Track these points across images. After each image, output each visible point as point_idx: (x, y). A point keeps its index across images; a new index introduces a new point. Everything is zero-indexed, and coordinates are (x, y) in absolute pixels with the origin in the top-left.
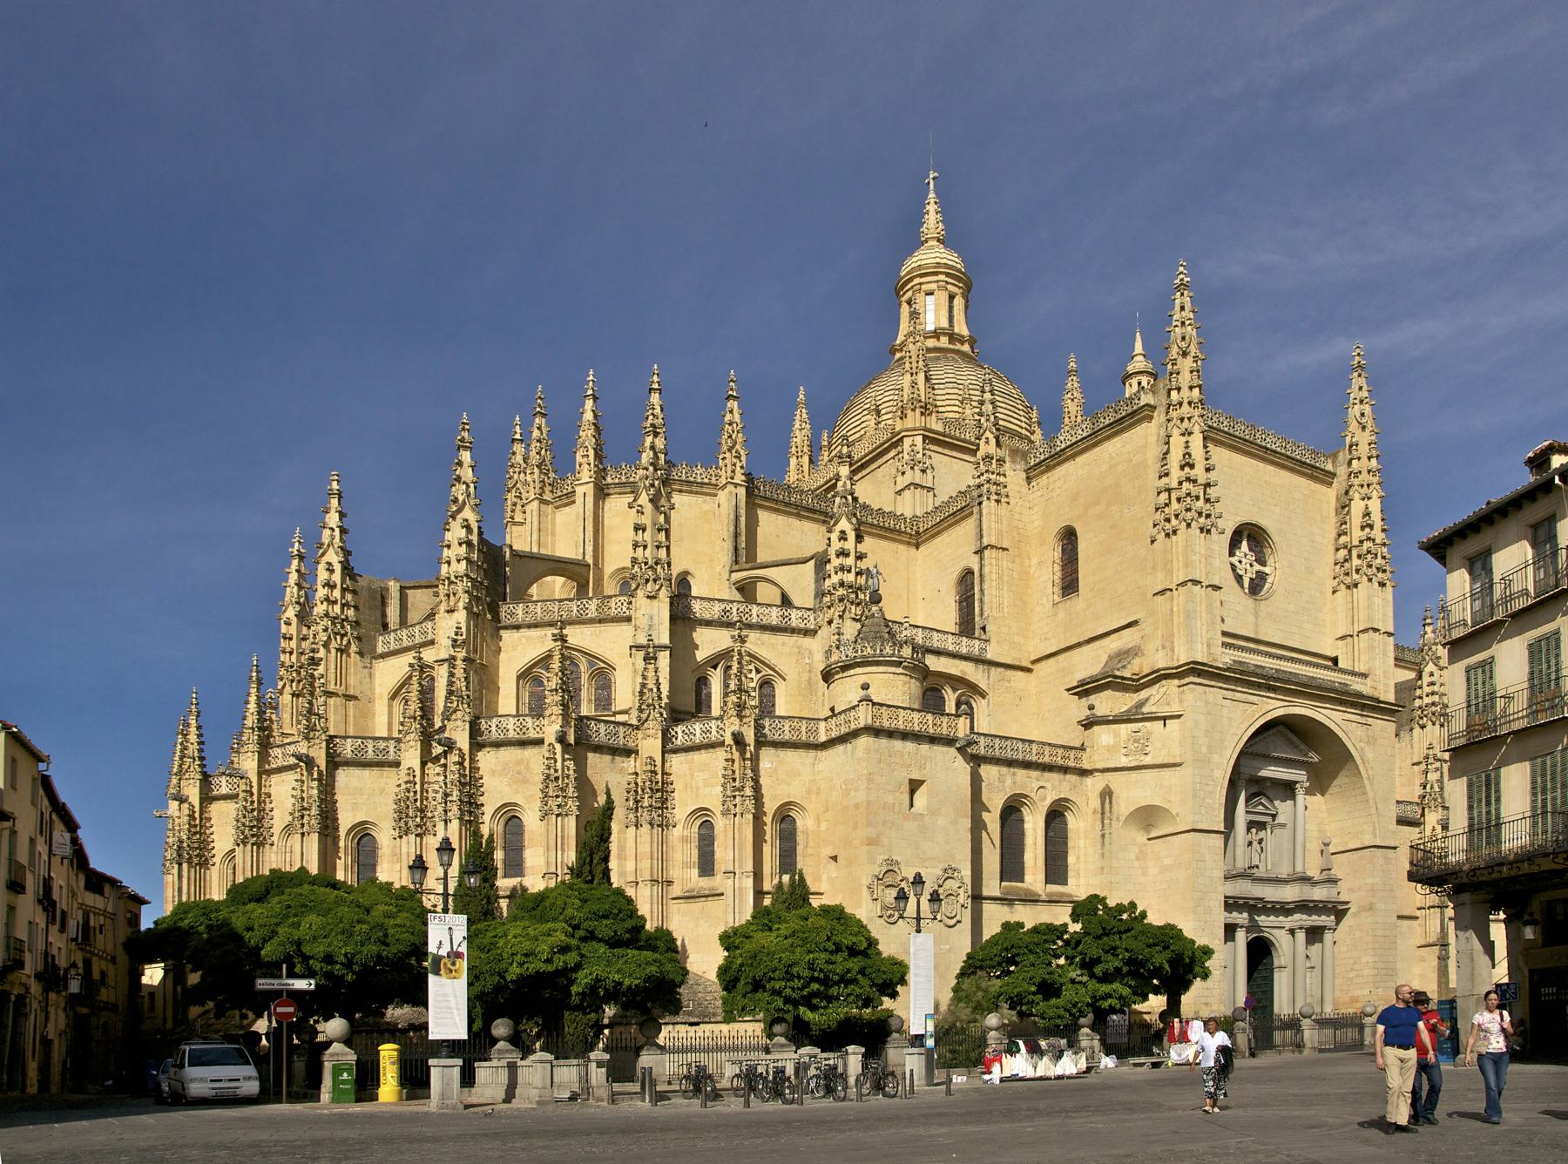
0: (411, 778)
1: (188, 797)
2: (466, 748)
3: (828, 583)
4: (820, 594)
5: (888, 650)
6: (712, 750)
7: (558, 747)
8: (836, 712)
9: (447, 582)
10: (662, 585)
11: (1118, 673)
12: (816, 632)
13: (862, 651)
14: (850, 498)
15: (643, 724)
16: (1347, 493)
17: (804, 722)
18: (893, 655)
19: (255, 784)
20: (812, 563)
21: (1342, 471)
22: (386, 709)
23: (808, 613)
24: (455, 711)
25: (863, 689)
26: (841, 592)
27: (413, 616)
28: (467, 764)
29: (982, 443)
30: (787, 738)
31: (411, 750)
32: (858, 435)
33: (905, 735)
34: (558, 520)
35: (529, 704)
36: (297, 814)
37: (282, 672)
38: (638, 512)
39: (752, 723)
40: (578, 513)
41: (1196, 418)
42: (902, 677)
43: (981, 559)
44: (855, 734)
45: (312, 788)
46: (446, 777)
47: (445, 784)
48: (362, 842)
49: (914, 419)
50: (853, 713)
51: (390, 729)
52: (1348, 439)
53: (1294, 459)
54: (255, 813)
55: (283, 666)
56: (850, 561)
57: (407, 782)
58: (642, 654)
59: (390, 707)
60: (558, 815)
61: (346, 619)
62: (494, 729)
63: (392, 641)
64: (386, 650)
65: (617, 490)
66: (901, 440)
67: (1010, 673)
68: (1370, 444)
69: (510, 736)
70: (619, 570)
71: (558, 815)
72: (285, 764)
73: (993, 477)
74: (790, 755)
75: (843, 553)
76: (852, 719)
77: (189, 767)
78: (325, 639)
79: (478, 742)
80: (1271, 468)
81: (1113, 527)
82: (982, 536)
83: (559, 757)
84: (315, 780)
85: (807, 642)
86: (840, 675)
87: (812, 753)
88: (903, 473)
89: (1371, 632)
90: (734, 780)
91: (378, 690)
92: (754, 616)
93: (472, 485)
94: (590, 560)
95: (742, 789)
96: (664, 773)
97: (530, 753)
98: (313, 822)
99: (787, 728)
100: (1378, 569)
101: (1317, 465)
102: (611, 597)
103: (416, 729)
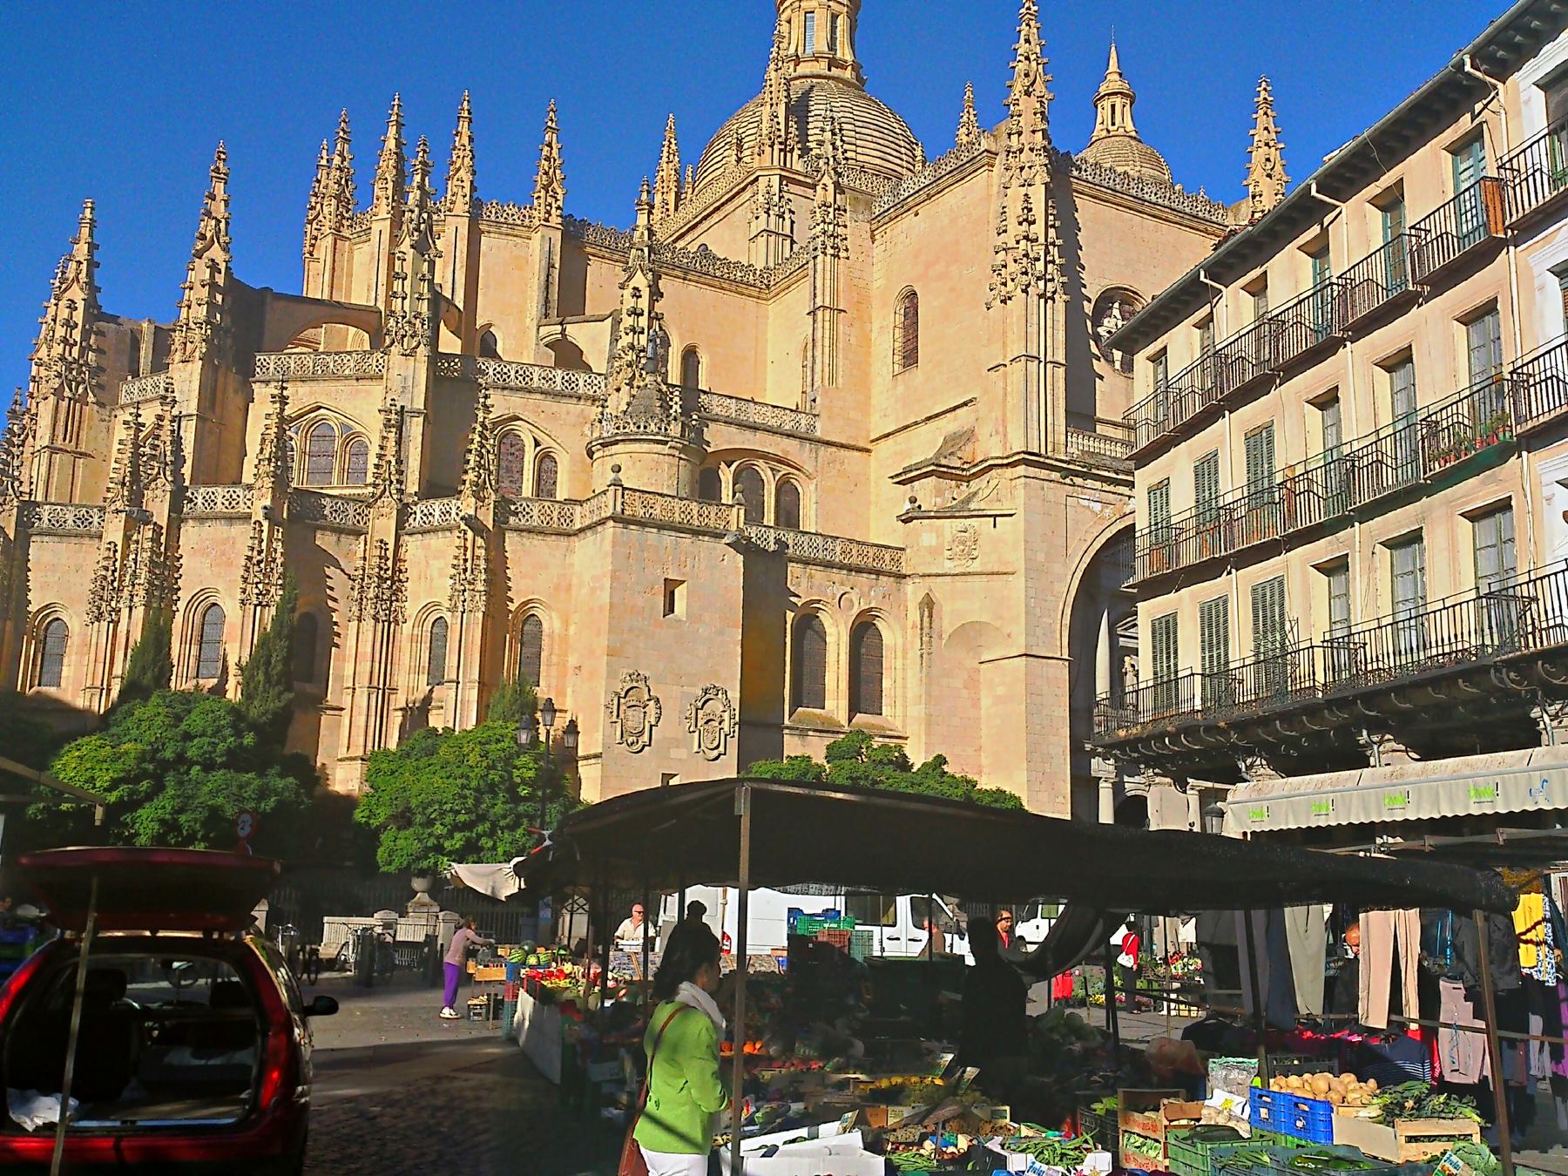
9: (184, 329)
11: (943, 462)
32: (718, 172)
39: (492, 506)
41: (1038, 167)
44: (602, 522)
48: (51, 628)
66: (756, 179)
67: (843, 452)
76: (603, 505)
81: (952, 289)
88: (757, 218)
96: (396, 559)
99: (535, 513)
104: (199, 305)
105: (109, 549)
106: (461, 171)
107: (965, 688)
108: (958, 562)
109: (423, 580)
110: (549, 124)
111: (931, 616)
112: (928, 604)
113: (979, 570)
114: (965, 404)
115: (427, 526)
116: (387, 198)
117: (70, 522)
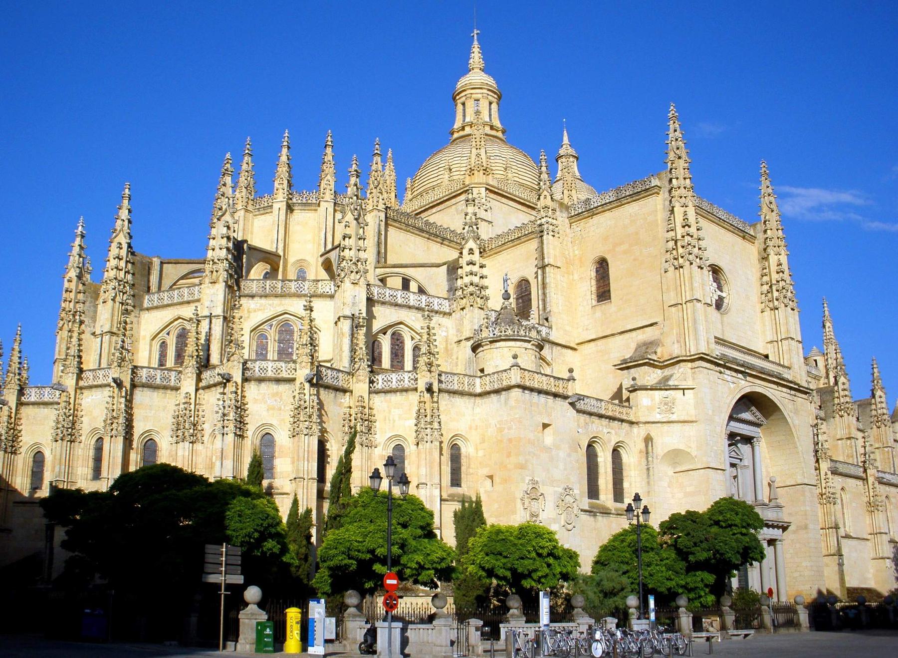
1: (8, 402)
2: (239, 381)
3: (459, 283)
4: (452, 290)
5: (522, 333)
6: (404, 393)
7: (307, 385)
8: (486, 373)
10: (361, 276)
13: (505, 332)
14: (475, 227)
15: (356, 372)
16: (765, 250)
17: (466, 378)
18: (525, 336)
19: (72, 396)
20: (445, 267)
21: (761, 236)
22: (148, 347)
24: (233, 355)
25: (514, 358)
26: (472, 289)
27: (166, 283)
28: (239, 392)
29: (542, 198)
30: (456, 389)
32: (435, 183)
33: (540, 392)
34: (255, 224)
35: (256, 351)
36: (109, 422)
37: (63, 315)
38: (346, 226)
40: (274, 221)
42: (531, 351)
43: (544, 273)
44: (508, 388)
45: (121, 403)
47: (224, 407)
49: (479, 177)
50: (505, 374)
51: (149, 362)
52: (762, 217)
53: (734, 226)
54: (71, 418)
55: (64, 310)
56: (475, 269)
57: (184, 403)
59: (151, 346)
60: (305, 435)
61: (127, 282)
62: (257, 369)
64: (151, 306)
65: (300, 208)
68: (777, 221)
69: (269, 375)
70: (298, 261)
71: (305, 435)
72: (95, 383)
73: (550, 220)
74: (458, 401)
75: (471, 263)
76: (504, 378)
77: (11, 381)
78: (114, 295)
79: (245, 380)
80: (723, 231)
81: (635, 260)
82: (543, 258)
83: (306, 391)
84: (123, 397)
85: (444, 321)
86: (489, 347)
87: (472, 399)
89: (790, 339)
90: (426, 416)
91: (142, 333)
92: (411, 300)
93: (231, 199)
94: (281, 254)
95: (431, 423)
97: (283, 388)
100: (790, 300)
101: (746, 231)
102: (318, 281)
103: (193, 364)
104: (221, 249)
105: (187, 397)
106: (329, 176)
107: (669, 487)
108: (665, 415)
109: (387, 421)
110: (376, 152)
111: (652, 446)
112: (648, 440)
113: (677, 420)
114: (651, 325)
115: (388, 388)
116: (284, 189)
117: (158, 379)
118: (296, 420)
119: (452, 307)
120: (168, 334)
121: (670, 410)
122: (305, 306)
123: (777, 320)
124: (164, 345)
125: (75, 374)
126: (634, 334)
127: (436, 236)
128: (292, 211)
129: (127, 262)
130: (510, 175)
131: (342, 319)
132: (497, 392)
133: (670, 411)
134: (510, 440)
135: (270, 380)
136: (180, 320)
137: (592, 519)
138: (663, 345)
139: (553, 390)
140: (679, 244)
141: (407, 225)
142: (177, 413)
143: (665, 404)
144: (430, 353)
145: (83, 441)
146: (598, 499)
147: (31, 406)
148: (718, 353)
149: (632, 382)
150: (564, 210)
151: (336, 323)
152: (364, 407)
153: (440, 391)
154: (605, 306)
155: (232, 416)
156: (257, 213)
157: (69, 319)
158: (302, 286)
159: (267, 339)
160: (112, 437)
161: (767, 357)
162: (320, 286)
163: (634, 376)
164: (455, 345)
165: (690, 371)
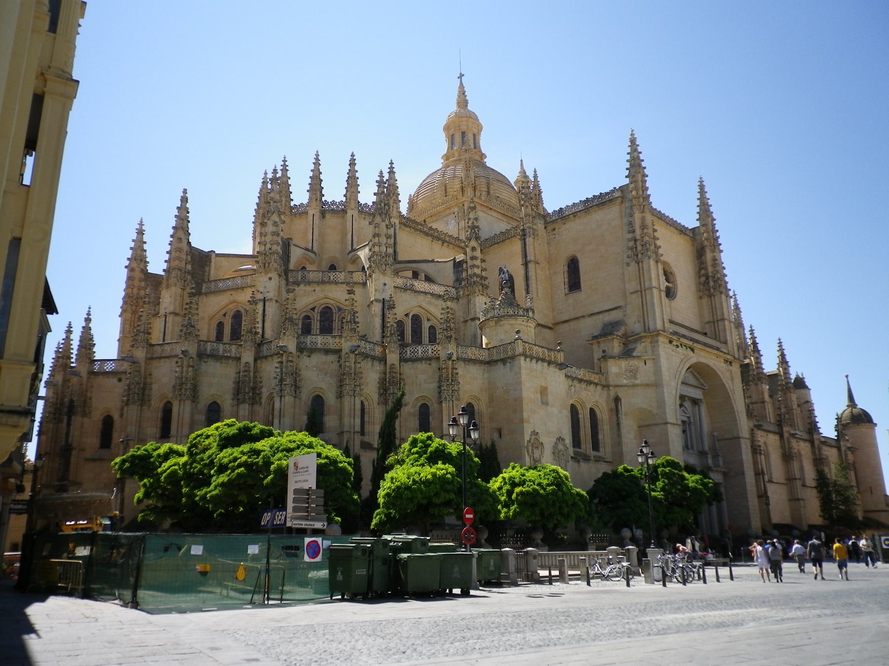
0: (248, 369)
1: (80, 373)
3: (464, 275)
4: (458, 280)
7: (352, 356)
12: (458, 299)
23: (453, 290)
31: (248, 352)
33: (538, 359)
36: (177, 387)
38: (375, 227)
46: (282, 369)
56: (478, 262)
58: (380, 305)
59: (209, 325)
63: (213, 287)
65: (330, 214)
73: (531, 225)
76: (509, 350)
82: (526, 256)
84: (189, 366)
87: (483, 367)
90: (448, 380)
96: (400, 374)
97: (331, 358)
98: (188, 393)
109: (415, 385)
112: (617, 400)
118: (342, 384)
119: (459, 294)
120: (224, 315)
121: (634, 377)
122: (348, 290)
123: (714, 305)
124: (220, 325)
125: (145, 349)
126: (601, 316)
127: (438, 239)
128: (324, 217)
129: (187, 255)
130: (491, 192)
131: (374, 303)
132: (504, 361)
133: (636, 379)
134: (516, 400)
135: (320, 350)
136: (235, 304)
137: (576, 464)
138: (626, 325)
139: (547, 359)
140: (638, 243)
141: (416, 230)
142: (237, 380)
143: (631, 371)
144: (451, 329)
145: (153, 405)
146: (580, 447)
147: (101, 376)
148: (671, 331)
149: (603, 354)
150: (541, 218)
151: (369, 306)
152: (396, 373)
153: (458, 359)
154: (576, 295)
155: (289, 380)
156: (294, 218)
157: (132, 303)
158: (339, 276)
159: (311, 319)
160: (180, 400)
161: (706, 334)
162: (354, 276)
163: (604, 348)
164: (462, 325)
165: (649, 345)
